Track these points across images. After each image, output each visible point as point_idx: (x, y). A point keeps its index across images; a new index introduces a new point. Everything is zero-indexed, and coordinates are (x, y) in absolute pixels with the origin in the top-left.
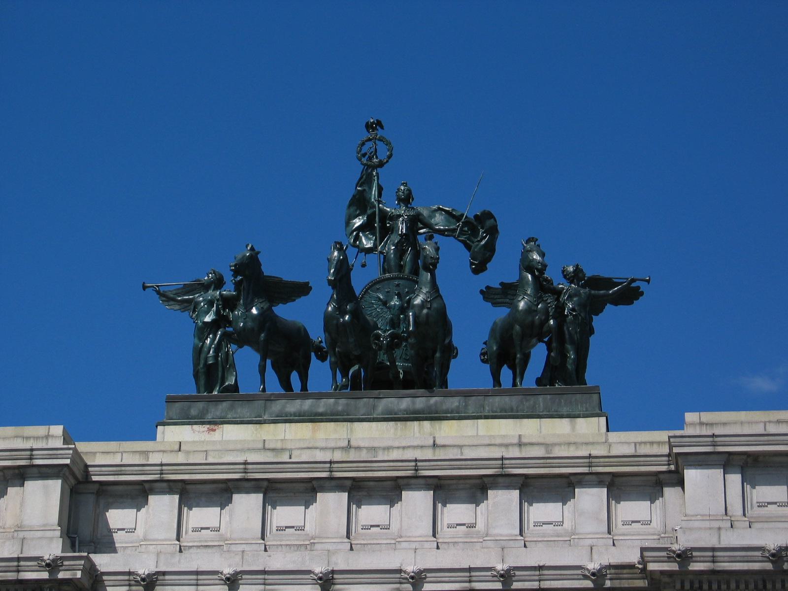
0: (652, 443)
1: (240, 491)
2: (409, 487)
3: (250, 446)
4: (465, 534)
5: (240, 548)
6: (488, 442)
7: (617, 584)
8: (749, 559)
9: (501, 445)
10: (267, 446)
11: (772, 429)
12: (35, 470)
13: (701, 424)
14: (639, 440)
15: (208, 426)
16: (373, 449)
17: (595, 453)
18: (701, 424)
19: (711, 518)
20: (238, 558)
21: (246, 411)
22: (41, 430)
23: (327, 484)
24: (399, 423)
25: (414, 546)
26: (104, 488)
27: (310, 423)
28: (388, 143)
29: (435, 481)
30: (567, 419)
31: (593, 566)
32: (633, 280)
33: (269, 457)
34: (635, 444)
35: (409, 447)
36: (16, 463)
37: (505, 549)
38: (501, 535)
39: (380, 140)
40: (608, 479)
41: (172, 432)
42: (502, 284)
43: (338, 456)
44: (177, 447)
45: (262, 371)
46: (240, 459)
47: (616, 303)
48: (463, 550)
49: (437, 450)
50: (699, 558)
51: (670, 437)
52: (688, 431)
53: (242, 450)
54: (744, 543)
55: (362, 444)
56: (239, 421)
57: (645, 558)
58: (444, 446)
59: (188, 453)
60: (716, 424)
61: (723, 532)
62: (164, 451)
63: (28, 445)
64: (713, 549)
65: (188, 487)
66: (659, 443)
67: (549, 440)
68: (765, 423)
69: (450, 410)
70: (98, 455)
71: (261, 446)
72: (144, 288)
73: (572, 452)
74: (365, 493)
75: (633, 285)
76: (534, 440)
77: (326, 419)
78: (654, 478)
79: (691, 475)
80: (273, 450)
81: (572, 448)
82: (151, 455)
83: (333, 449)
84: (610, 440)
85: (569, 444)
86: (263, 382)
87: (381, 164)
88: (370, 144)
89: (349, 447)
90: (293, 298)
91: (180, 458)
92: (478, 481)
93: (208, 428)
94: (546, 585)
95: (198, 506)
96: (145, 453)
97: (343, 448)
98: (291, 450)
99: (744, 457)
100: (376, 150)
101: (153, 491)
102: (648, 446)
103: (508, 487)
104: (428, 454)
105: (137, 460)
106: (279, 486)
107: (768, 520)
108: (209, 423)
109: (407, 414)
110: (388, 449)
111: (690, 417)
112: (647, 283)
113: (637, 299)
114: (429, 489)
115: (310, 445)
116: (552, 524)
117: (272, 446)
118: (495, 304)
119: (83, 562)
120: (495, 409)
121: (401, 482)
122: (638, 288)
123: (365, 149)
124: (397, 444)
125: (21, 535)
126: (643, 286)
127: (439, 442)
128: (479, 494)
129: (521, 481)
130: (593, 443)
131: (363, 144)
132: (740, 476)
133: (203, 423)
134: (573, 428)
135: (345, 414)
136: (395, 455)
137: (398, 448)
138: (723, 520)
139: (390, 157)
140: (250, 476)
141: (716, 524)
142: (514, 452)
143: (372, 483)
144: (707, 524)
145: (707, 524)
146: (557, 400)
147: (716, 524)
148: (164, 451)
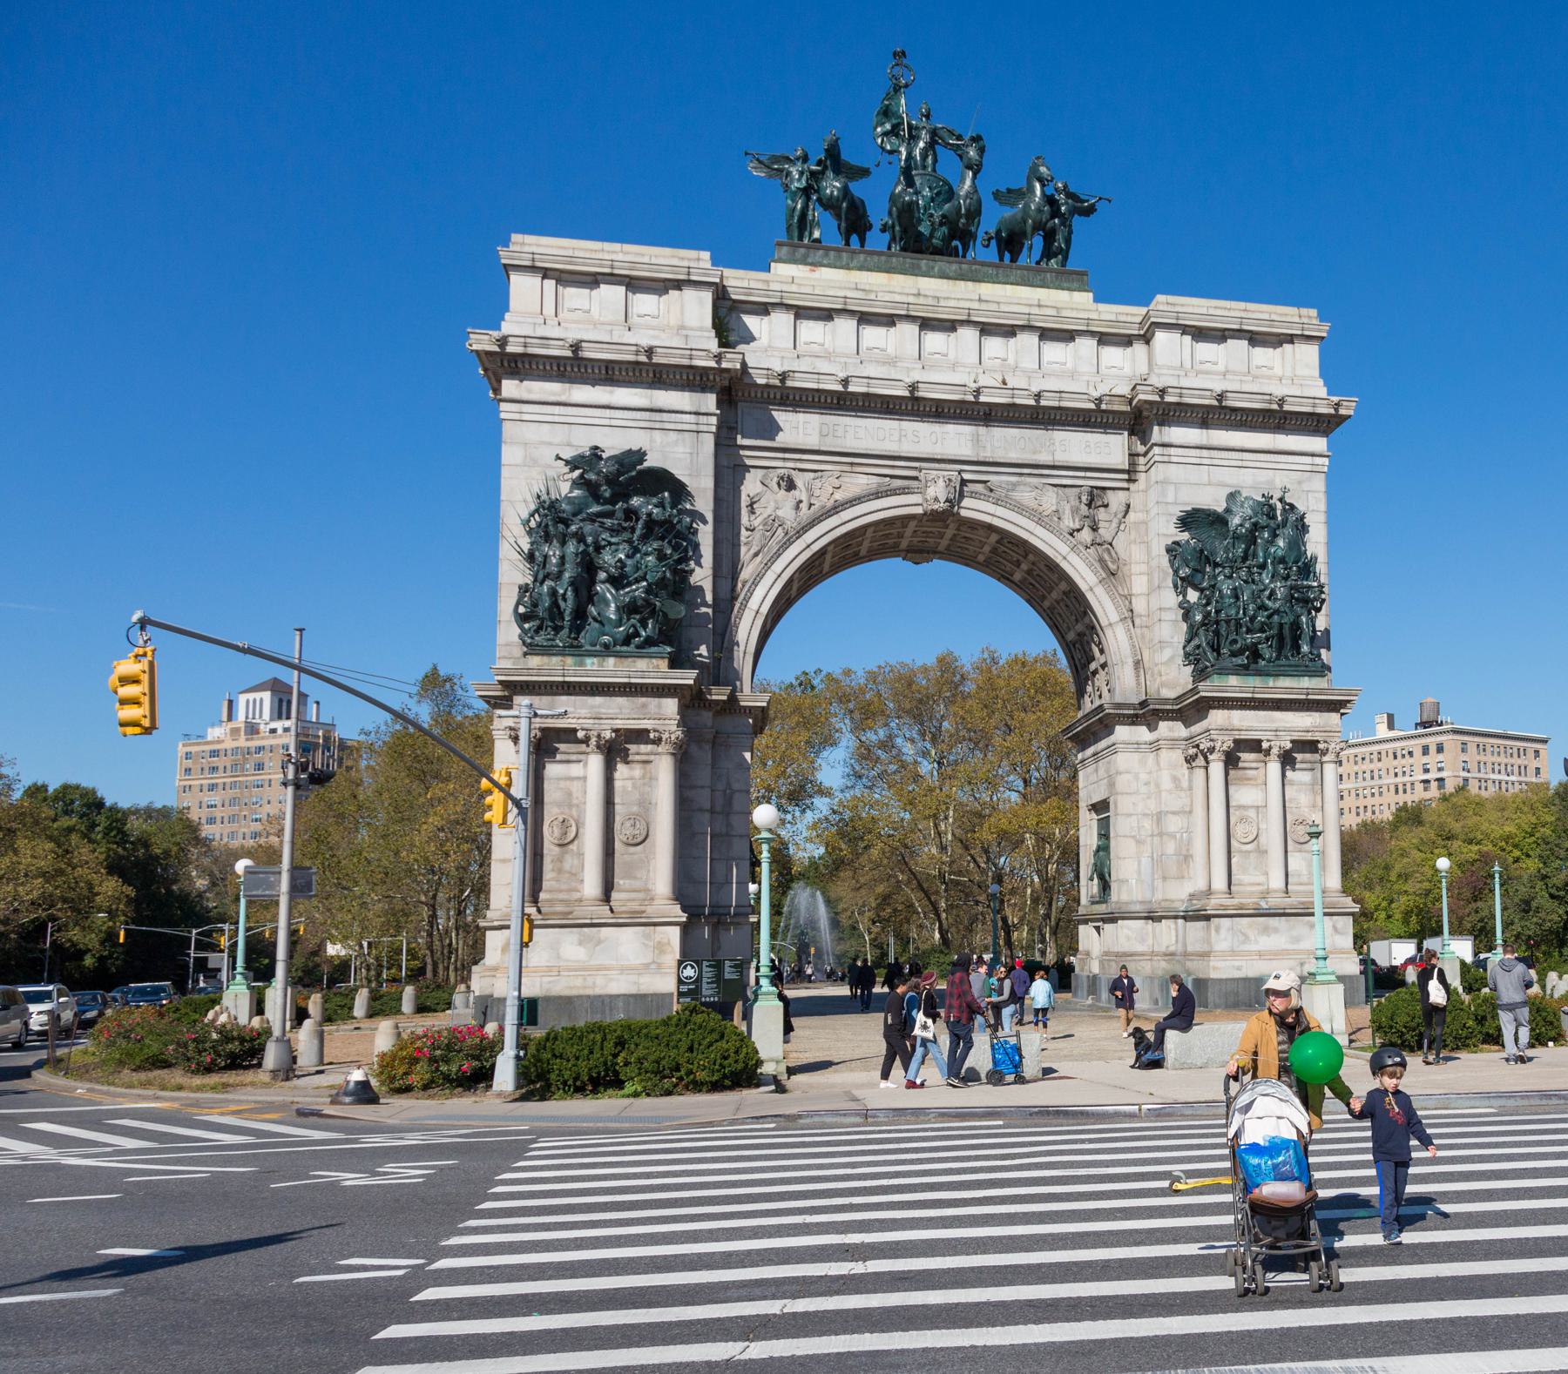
5: (842, 360)
7: (1110, 407)
11: (1212, 311)
31: (1096, 394)
43: (911, 299)
46: (842, 294)
53: (840, 288)
55: (928, 293)
67: (1059, 305)
79: (1160, 337)
94: (1064, 404)
104: (976, 305)
107: (1207, 373)
127: (983, 298)
136: (952, 303)
142: (1035, 310)
144: (1171, 372)
145: (1171, 372)
147: (1177, 373)
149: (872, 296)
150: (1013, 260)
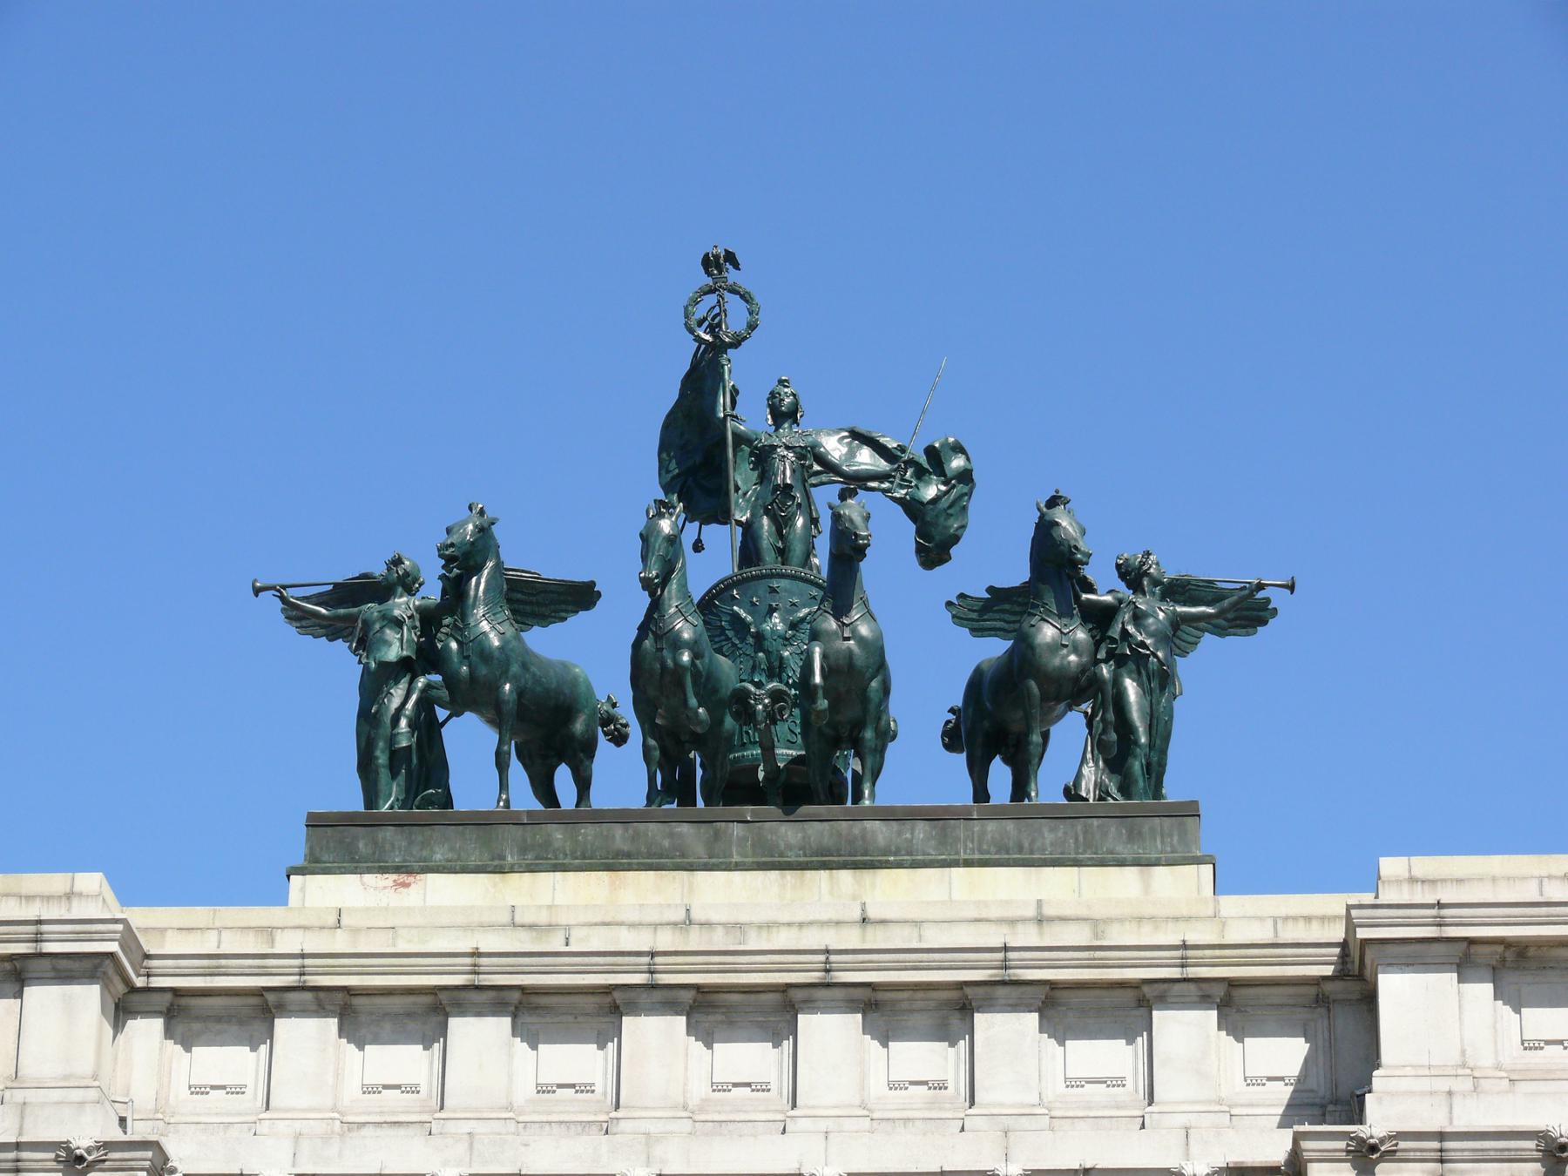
0: (1308, 919)
1: (463, 1010)
2: (811, 1006)
3: (486, 918)
4: (928, 1103)
5: (466, 1127)
6: (976, 915)
8: (1513, 1155)
9: (1000, 921)
10: (518, 919)
12: (46, 964)
13: (1412, 880)
14: (1283, 912)
15: (394, 877)
16: (738, 927)
17: (1192, 939)
18: (1412, 880)
19: (1433, 1073)
20: (462, 1148)
21: (473, 846)
22: (56, 882)
23: (644, 998)
24: (788, 874)
25: (823, 1125)
26: (184, 1001)
27: (605, 873)
28: (746, 298)
29: (867, 993)
30: (1132, 868)
32: (1261, 587)
34: (1275, 920)
35: (811, 923)
36: (6, 948)
37: (1009, 1134)
38: (1002, 1105)
39: (733, 291)
40: (1219, 992)
41: (321, 887)
42: (991, 589)
43: (665, 941)
44: (332, 920)
45: (502, 764)
47: (1221, 632)
48: (924, 1134)
50: (1412, 1154)
51: (1349, 908)
52: (1388, 895)
53: (467, 928)
54: (1491, 1124)
55: (715, 917)
56: (458, 868)
57: (1304, 1154)
58: (883, 922)
59: (355, 931)
60: (1443, 881)
61: (1457, 1100)
62: (305, 928)
63: (31, 913)
64: (1441, 1136)
65: (357, 1001)
66: (1323, 919)
67: (1099, 912)
68: (1541, 879)
69: (893, 849)
70: (169, 933)
73: (1147, 937)
74: (720, 1017)
75: (1261, 595)
76: (1068, 912)
77: (638, 863)
78: (1312, 990)
80: (531, 927)
81: (1147, 928)
82: (278, 935)
83: (656, 926)
84: (1223, 913)
85: (1140, 919)
86: (503, 785)
87: (737, 342)
88: (711, 299)
89: (688, 922)
90: (563, 614)
91: (340, 943)
92: (954, 995)
93: (395, 881)
95: (377, 1040)
96: (269, 931)
97: (675, 924)
98: (568, 928)
99: (1500, 949)
101: (283, 1010)
102: (1301, 923)
103: (1015, 1007)
104: (851, 938)
105: (251, 945)
106: (544, 1000)
108: (397, 870)
109: (805, 856)
110: (769, 926)
111: (1391, 866)
113: (1264, 622)
114: (853, 1011)
115: (607, 919)
116: (1106, 1082)
117: (528, 918)
118: (977, 631)
119: (149, 1154)
120: (985, 847)
121: (798, 995)
122: (1268, 601)
124: (786, 918)
125: (19, 1096)
126: (1277, 598)
127: (872, 913)
128: (955, 1021)
129: (1041, 993)
130: (1188, 919)
132: (1491, 986)
133: (383, 870)
134: (1147, 888)
135: (678, 854)
136: (782, 940)
137: (789, 924)
138: (1456, 1076)
139: (752, 327)
140: (485, 980)
141: (1443, 1085)
144: (1425, 1084)
145: (1425, 1084)
146: (1113, 829)
147: (1443, 1085)
148: (305, 928)
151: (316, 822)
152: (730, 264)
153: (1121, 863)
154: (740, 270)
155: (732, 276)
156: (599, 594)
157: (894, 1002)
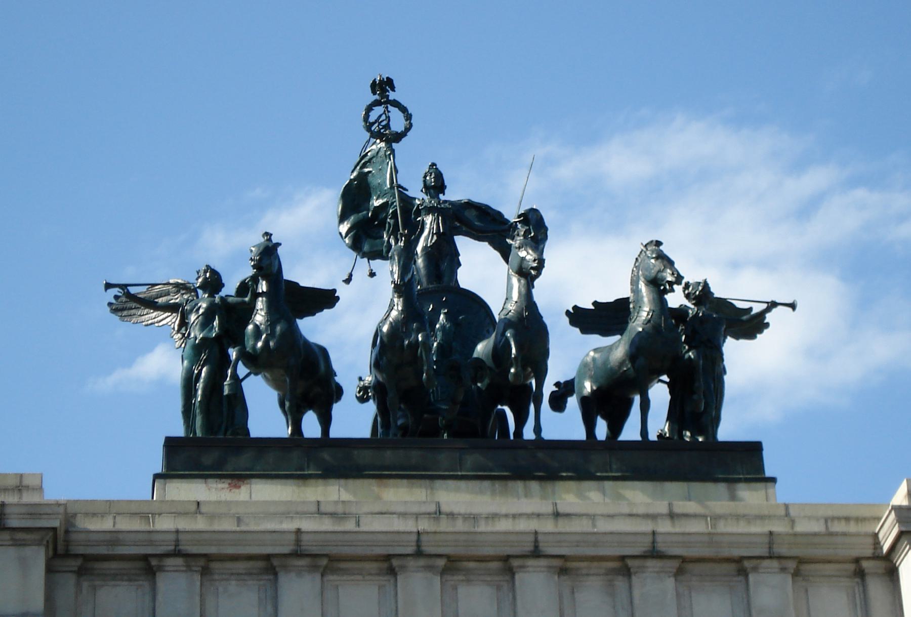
10: (323, 509)
28: (403, 109)
33: (327, 525)
41: (178, 488)
42: (595, 303)
43: (424, 525)
44: (193, 508)
49: (561, 522)
55: (456, 509)
58: (568, 515)
59: (212, 517)
71: (313, 508)
72: (108, 286)
74: (461, 577)
80: (333, 515)
83: (417, 516)
87: (398, 137)
88: (378, 111)
91: (200, 524)
100: (388, 118)
102: (843, 523)
106: (343, 565)
112: (790, 309)
113: (761, 332)
115: (384, 510)
117: (330, 509)
118: (584, 331)
123: (372, 119)
127: (561, 509)
131: (369, 109)
136: (504, 526)
139: (408, 129)
142: (664, 527)
143: (472, 565)
149: (350, 526)
150: (616, 427)
151: (171, 444)
152: (389, 87)
153: (716, 480)
154: (395, 91)
155: (392, 96)
156: (338, 298)
157: (578, 569)
